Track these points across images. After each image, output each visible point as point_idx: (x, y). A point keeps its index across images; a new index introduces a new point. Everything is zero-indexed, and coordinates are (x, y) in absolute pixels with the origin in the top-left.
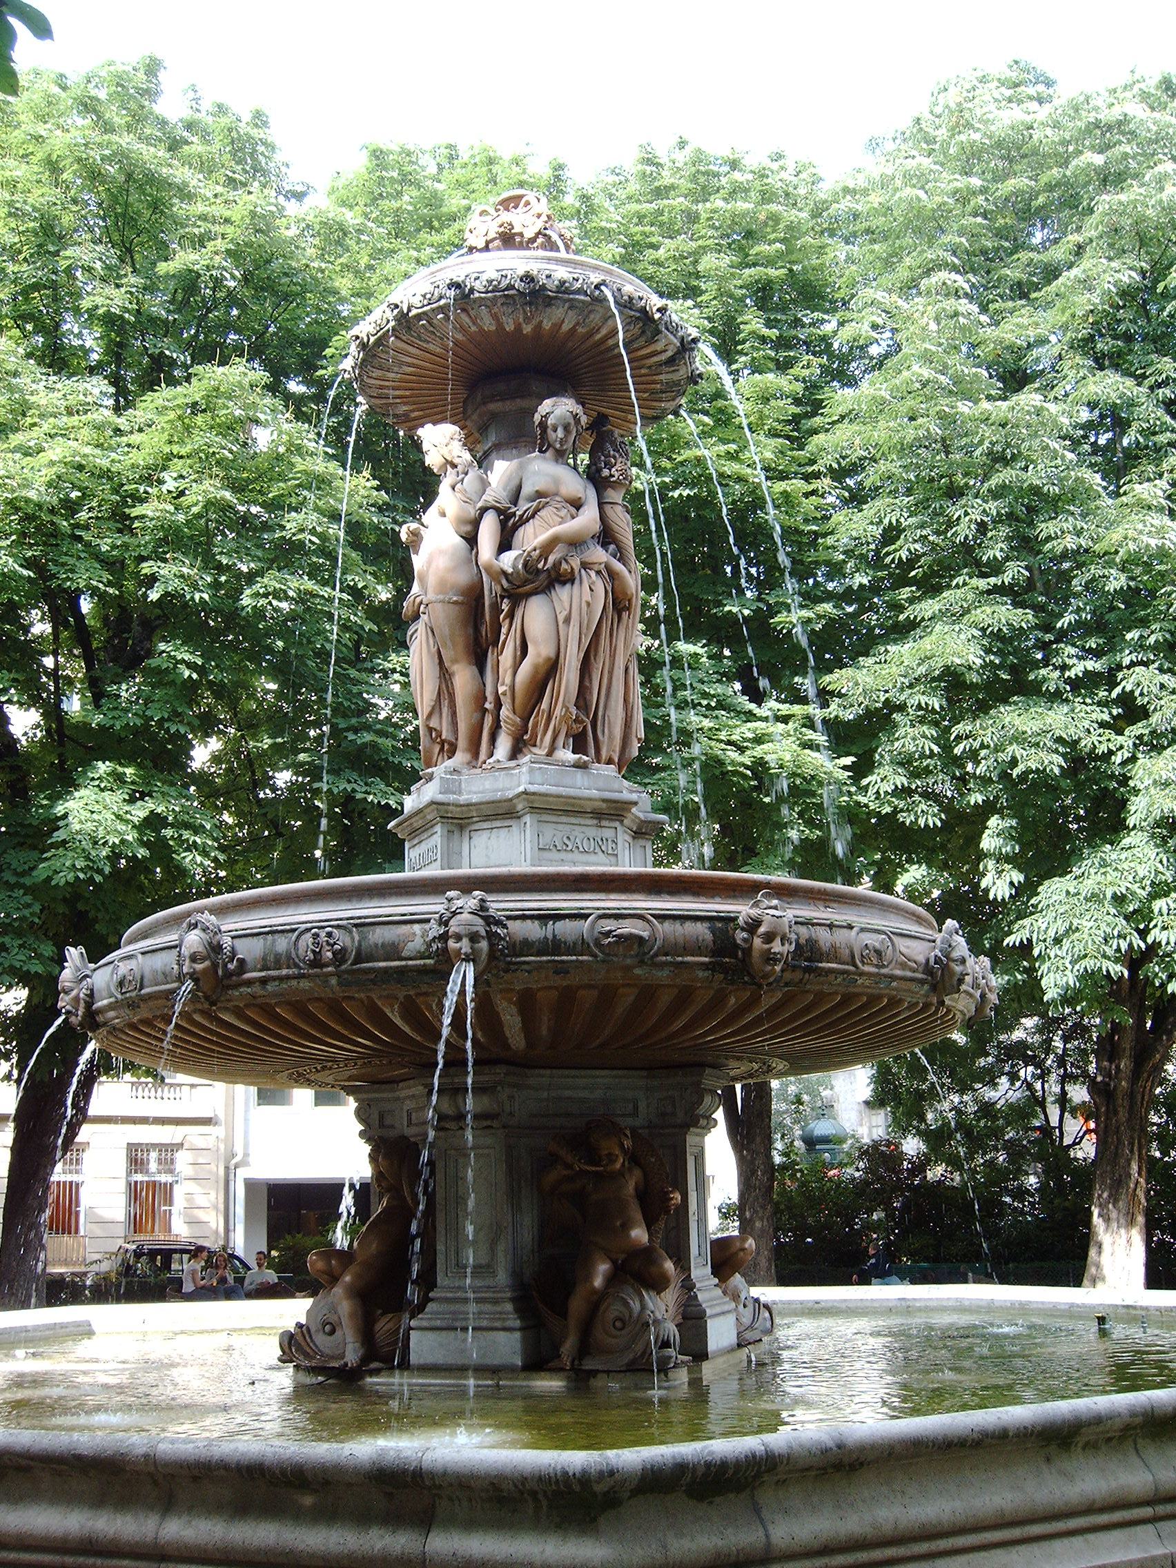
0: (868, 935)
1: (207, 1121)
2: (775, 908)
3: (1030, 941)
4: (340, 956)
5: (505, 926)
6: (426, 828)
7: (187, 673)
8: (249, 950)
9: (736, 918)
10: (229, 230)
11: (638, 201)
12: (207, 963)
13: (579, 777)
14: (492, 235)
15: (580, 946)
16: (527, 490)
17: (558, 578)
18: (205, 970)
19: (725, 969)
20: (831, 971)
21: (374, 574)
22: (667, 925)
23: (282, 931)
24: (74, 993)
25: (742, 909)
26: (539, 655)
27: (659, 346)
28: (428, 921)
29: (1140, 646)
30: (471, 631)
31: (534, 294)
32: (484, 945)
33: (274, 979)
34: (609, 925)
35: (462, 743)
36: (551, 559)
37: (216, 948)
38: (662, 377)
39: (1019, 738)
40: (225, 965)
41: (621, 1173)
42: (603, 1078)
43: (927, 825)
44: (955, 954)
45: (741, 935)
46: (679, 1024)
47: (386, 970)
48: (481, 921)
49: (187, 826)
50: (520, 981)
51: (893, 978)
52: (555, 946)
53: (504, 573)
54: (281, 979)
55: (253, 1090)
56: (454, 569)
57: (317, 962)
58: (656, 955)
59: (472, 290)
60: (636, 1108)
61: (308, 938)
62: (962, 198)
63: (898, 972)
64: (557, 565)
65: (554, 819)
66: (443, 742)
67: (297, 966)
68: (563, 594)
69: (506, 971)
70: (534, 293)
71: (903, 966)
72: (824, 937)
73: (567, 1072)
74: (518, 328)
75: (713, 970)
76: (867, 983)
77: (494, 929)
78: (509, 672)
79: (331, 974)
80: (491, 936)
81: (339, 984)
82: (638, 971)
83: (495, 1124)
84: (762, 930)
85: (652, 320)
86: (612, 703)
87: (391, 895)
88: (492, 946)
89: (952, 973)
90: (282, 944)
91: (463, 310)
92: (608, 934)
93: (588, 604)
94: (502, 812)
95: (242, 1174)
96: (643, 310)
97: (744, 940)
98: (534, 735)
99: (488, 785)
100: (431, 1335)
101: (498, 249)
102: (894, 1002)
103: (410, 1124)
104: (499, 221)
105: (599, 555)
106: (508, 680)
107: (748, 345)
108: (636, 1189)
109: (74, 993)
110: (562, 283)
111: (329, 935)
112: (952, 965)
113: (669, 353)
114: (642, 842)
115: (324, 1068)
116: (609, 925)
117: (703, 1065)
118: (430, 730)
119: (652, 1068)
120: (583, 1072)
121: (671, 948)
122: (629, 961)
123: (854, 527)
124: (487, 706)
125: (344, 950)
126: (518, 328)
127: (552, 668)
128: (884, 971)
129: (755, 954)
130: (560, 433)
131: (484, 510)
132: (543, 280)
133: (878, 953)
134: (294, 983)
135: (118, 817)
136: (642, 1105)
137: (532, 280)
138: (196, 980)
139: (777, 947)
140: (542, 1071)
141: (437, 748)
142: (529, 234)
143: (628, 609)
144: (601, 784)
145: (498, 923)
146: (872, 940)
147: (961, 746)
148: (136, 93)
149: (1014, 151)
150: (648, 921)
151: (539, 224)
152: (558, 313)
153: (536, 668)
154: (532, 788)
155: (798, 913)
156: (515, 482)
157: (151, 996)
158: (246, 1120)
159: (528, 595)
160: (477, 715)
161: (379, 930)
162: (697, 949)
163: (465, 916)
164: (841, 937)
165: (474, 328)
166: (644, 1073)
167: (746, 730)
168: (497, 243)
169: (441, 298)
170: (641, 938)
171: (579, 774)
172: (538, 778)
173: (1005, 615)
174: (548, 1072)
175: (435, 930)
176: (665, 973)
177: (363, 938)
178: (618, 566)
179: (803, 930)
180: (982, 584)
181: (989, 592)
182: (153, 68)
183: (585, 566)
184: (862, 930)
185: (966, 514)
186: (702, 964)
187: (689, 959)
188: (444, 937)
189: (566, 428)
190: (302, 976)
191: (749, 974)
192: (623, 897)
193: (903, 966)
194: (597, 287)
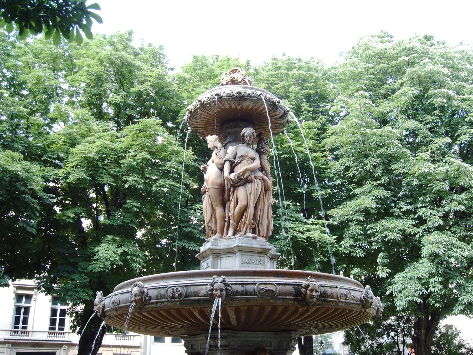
1: (138, 347)
2: (314, 281)
3: (392, 292)
4: (180, 295)
5: (231, 287)
6: (208, 256)
7: (136, 209)
8: (153, 293)
9: (301, 285)
10: (151, 79)
11: (272, 71)
12: (140, 297)
13: (254, 241)
14: (229, 80)
15: (254, 293)
16: (238, 155)
17: (248, 181)
18: (139, 299)
19: (298, 300)
22: (281, 287)
23: (163, 288)
24: (98, 306)
25: (304, 282)
26: (242, 204)
27: (278, 113)
28: (207, 285)
29: (424, 202)
30: (221, 197)
31: (241, 98)
32: (224, 292)
33: (160, 302)
34: (262, 286)
35: (218, 231)
36: (246, 175)
37: (142, 293)
38: (278, 122)
39: (387, 229)
40: (145, 298)
42: (261, 334)
43: (360, 256)
44: (369, 296)
45: (303, 290)
46: (284, 317)
47: (194, 300)
48: (223, 285)
49: (134, 255)
50: (235, 304)
51: (350, 303)
52: (246, 293)
53: (231, 180)
54: (162, 302)
55: (153, 337)
56: (217, 178)
57: (173, 297)
58: (277, 296)
59: (222, 96)
60: (271, 344)
61: (171, 289)
62: (367, 69)
63: (352, 302)
64: (247, 177)
65: (246, 254)
66: (212, 231)
67: (167, 298)
68: (249, 186)
69: (231, 300)
70: (241, 97)
71: (353, 300)
72: (329, 290)
73: (249, 332)
74: (236, 107)
75: (295, 301)
77: (227, 287)
78: (233, 210)
79: (177, 301)
80: (226, 289)
81: (180, 304)
82: (271, 301)
83: (227, 348)
84: (310, 288)
85: (276, 105)
86: (264, 219)
87: (196, 277)
88: (227, 293)
89: (368, 302)
90: (163, 291)
91: (220, 102)
92: (262, 289)
93: (257, 189)
94: (230, 252)
96: (273, 102)
97: (304, 291)
98: (240, 228)
99: (226, 243)
101: (230, 84)
102: (351, 311)
103: (201, 348)
104: (231, 76)
105: (260, 174)
106: (232, 212)
107: (304, 112)
109: (98, 306)
110: (249, 94)
111: (177, 289)
112: (368, 299)
113: (281, 115)
114: (273, 261)
115: (175, 330)
116: (262, 286)
117: (291, 331)
118: (209, 227)
119: (276, 331)
120: (255, 332)
121: (281, 294)
122: (269, 298)
123: (336, 167)
124: (226, 219)
125: (181, 293)
126: (236, 107)
127: (245, 208)
128: (347, 301)
129: (308, 296)
130: (248, 138)
131: (225, 161)
132: (243, 93)
133: (345, 295)
134: (166, 303)
135: (114, 252)
136: (273, 343)
137: (240, 93)
138: (136, 302)
139: (314, 293)
140: (242, 332)
141: (211, 232)
142: (239, 80)
143: (269, 190)
144: (260, 243)
145: (229, 286)
146: (344, 291)
147: (370, 231)
148: (125, 40)
149: (381, 56)
150: (275, 285)
151: (242, 77)
152: (248, 103)
153: (241, 208)
154: (239, 245)
155: (321, 283)
156: (235, 153)
157: (122, 307)
158: (150, 347)
159: (239, 186)
160: (223, 222)
161: (192, 287)
162: (290, 294)
163: (219, 283)
164: (334, 290)
165: (223, 107)
166: (273, 333)
167: (304, 228)
168: (230, 83)
169: (213, 98)
170: (272, 291)
171: (254, 240)
172: (241, 241)
173: (382, 192)
174: (244, 332)
175: (209, 288)
176: (280, 301)
177: (187, 290)
178: (265, 178)
179: (322, 288)
180: (375, 183)
181: (377, 186)
182: (130, 33)
183: (256, 177)
184: (341, 288)
185: (370, 162)
186: (292, 299)
188: (212, 290)
189: (250, 137)
190: (169, 301)
191: (306, 302)
192: (267, 278)
193: (353, 300)
194: (259, 95)
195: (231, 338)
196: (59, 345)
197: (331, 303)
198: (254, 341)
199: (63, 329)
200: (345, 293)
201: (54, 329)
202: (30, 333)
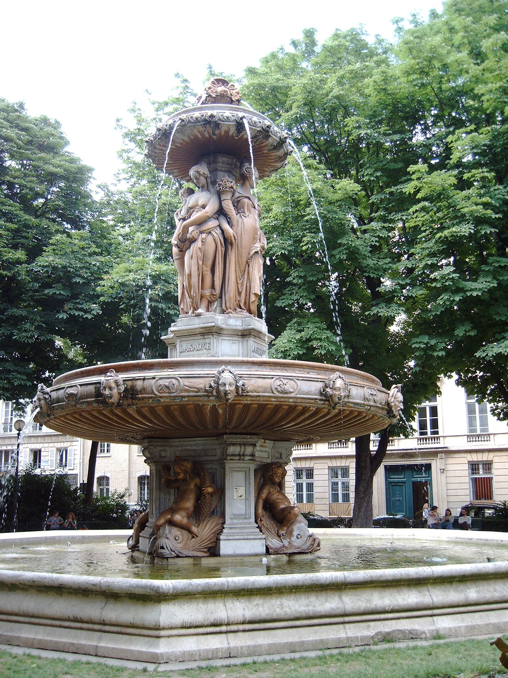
0: (164, 380)
20: (145, 398)
22: (83, 387)
25: (102, 378)
32: (43, 402)
41: (184, 480)
42: (199, 441)
72: (139, 384)
76: (167, 400)
100: (143, 539)
108: (196, 485)
120: (191, 439)
128: (173, 395)
132: (165, 127)
133: (167, 387)
144: (204, 321)
145: (47, 393)
146: (166, 382)
166: (215, 438)
174: (178, 440)
176: (84, 406)
179: (129, 383)
183: (201, 232)
184: (161, 379)
187: (89, 400)
195: (162, 448)
196: (434, 453)
198: (195, 450)
199: (437, 433)
200: (167, 384)
201: (426, 433)
202: (492, 436)
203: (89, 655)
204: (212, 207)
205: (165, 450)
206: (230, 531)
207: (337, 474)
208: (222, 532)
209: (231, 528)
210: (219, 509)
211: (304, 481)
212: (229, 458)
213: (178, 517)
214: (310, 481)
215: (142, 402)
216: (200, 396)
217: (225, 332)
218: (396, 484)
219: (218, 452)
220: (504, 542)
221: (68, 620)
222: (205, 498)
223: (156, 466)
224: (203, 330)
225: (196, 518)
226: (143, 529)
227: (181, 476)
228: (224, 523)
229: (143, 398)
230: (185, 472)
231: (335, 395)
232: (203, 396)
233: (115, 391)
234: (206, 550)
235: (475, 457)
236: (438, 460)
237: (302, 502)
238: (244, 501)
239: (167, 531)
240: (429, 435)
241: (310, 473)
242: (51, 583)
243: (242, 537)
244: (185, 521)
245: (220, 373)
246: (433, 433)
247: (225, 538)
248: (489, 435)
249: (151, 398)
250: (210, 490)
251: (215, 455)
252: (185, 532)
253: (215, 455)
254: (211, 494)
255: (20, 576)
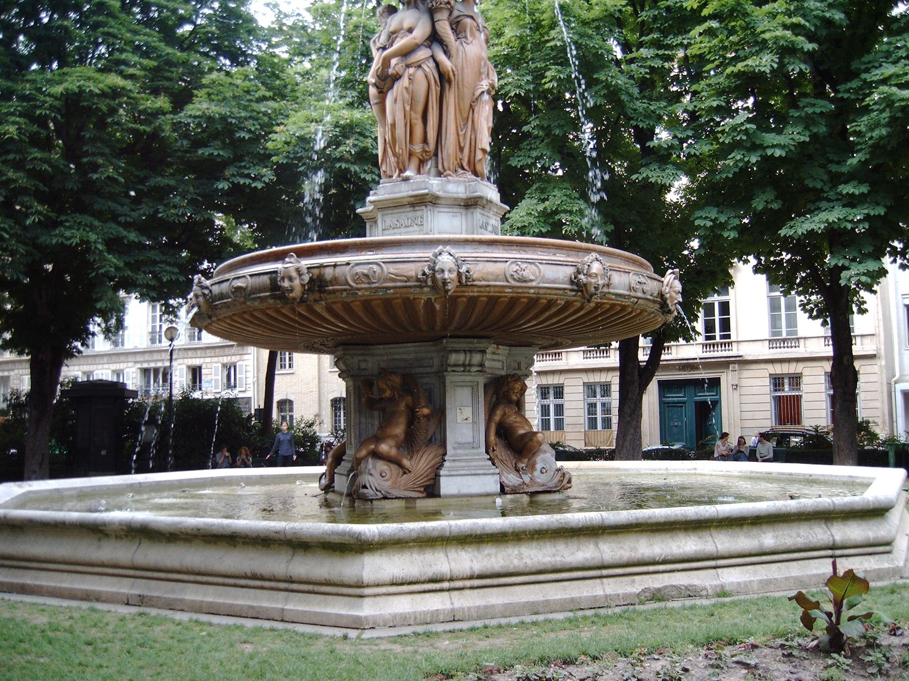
1: (873, 357)
20: (337, 290)
21: (812, 10)
22: (254, 278)
25: (278, 266)
32: (201, 299)
41: (391, 399)
42: (411, 347)
72: (329, 273)
76: (366, 293)
95: (901, 387)
108: (407, 406)
128: (373, 285)
133: (366, 276)
144: (414, 187)
145: (207, 288)
146: (364, 269)
158: (900, 354)
166: (432, 343)
174: (382, 346)
176: (256, 303)
183: (408, 66)
184: (357, 264)
187: (262, 295)
195: (360, 358)
196: (725, 364)
197: (338, 294)
198: (405, 360)
199: (729, 337)
200: (366, 272)
201: (714, 338)
202: (802, 341)
203: (274, 620)
204: (421, 31)
205: (365, 361)
206: (453, 464)
207: (595, 392)
208: (442, 465)
209: (454, 461)
210: (438, 436)
211: (551, 401)
212: (449, 369)
213: (384, 448)
214: (559, 401)
215: (332, 296)
216: (410, 287)
217: (442, 202)
218: (675, 405)
219: (436, 361)
220: (813, 477)
221: (245, 577)
222: (419, 422)
223: (354, 381)
224: (413, 199)
225: (408, 448)
226: (339, 464)
227: (388, 394)
228: (445, 454)
229: (335, 291)
230: (393, 388)
231: (591, 283)
232: (415, 286)
233: (297, 282)
234: (422, 489)
235: (778, 369)
236: (730, 373)
237: (549, 429)
238: (471, 426)
239: (370, 466)
240: (718, 339)
241: (559, 392)
242: (221, 531)
243: (468, 472)
244: (393, 452)
245: (436, 256)
246: (722, 337)
247: (447, 473)
248: (798, 339)
249: (345, 290)
250: (426, 411)
251: (432, 366)
252: (394, 467)
253: (432, 366)
254: (427, 417)
255: (180, 523)
